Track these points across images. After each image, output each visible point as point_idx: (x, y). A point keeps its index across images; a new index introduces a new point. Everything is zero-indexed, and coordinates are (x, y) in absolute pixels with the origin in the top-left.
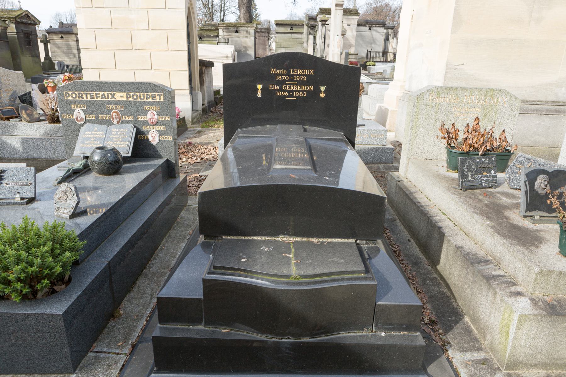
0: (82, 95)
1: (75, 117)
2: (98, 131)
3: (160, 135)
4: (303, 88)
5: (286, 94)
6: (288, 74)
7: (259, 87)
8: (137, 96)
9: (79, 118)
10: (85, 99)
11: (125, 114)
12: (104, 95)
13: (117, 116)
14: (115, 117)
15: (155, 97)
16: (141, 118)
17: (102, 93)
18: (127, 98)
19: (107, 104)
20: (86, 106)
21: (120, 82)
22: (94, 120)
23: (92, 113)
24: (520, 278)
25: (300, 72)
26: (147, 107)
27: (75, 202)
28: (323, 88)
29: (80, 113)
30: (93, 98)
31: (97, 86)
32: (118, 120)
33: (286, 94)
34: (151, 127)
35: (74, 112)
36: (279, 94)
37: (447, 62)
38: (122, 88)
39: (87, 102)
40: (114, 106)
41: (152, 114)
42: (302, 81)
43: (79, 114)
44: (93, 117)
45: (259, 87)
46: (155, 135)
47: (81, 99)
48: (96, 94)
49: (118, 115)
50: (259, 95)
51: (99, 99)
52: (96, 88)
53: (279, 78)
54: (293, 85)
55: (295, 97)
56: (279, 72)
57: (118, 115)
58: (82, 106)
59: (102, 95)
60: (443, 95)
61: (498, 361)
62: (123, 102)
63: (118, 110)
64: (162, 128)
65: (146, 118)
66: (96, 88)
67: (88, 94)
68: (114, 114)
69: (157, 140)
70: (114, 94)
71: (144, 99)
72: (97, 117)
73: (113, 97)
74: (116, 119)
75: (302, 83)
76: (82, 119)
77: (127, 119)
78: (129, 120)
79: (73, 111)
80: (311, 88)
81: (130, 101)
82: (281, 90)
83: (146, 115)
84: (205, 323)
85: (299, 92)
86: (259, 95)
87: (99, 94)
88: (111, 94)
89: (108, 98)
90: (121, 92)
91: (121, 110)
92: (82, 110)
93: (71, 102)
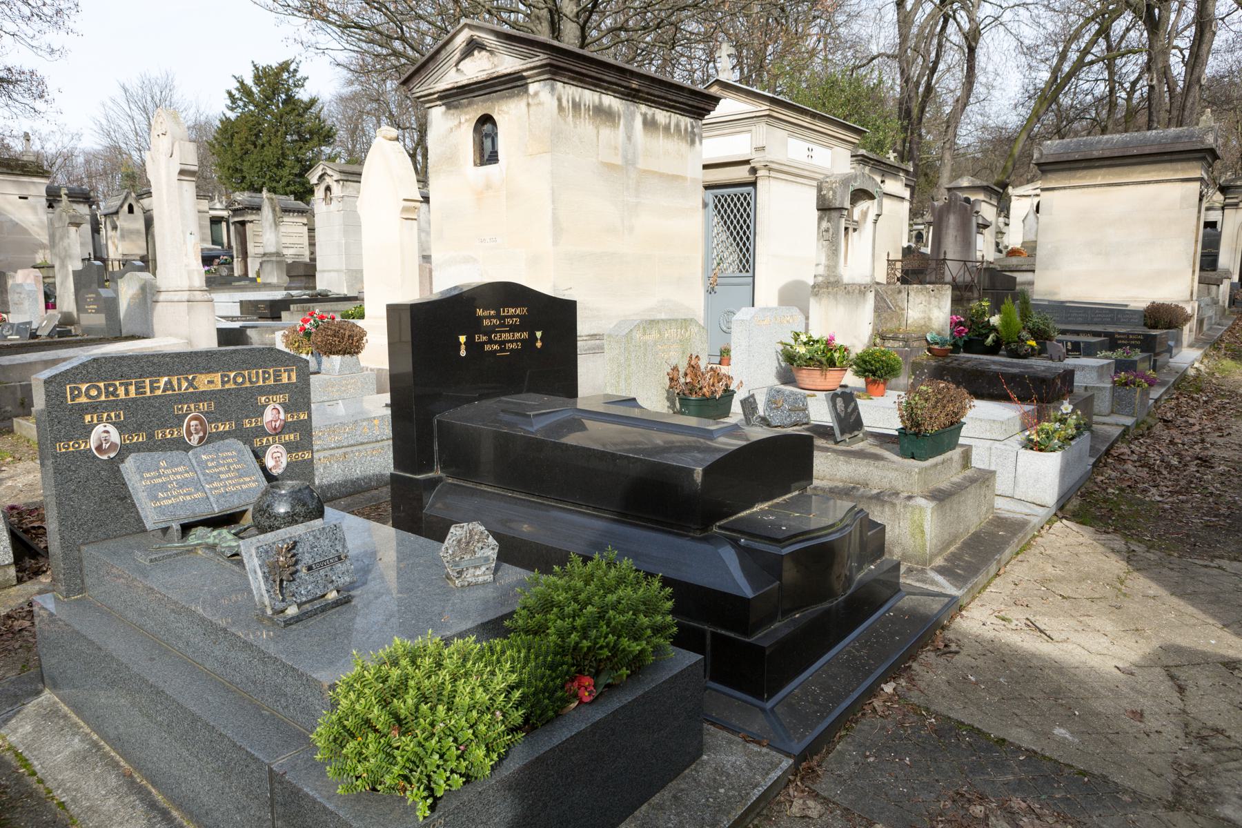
0: (116, 389)
1: (93, 443)
2: (172, 465)
3: (288, 452)
4: (517, 335)
5: (496, 347)
6: (498, 316)
7: (463, 339)
8: (244, 377)
9: (105, 446)
10: (122, 396)
11: (217, 420)
12: (170, 382)
13: (199, 427)
14: (196, 429)
15: (280, 375)
16: (251, 423)
17: (166, 379)
18: (223, 383)
19: (175, 403)
20: (124, 414)
21: (207, 352)
22: (142, 443)
23: (139, 429)
24: (899, 486)
25: (512, 311)
26: (263, 399)
27: (493, 549)
28: (539, 334)
29: (107, 432)
30: (142, 393)
31: (154, 364)
32: (201, 434)
33: (496, 347)
34: (271, 438)
35: (91, 432)
36: (487, 348)
37: (554, 286)
38: (211, 364)
39: (127, 405)
40: (192, 406)
41: (275, 411)
42: (515, 325)
43: (106, 435)
44: (141, 438)
45: (463, 339)
46: (279, 455)
47: (112, 398)
48: (151, 383)
49: (201, 424)
50: (463, 353)
51: (159, 392)
52: (151, 369)
53: (486, 323)
54: (505, 332)
55: (507, 351)
56: (486, 313)
57: (202, 423)
58: (113, 415)
59: (166, 384)
60: (648, 332)
61: (917, 564)
62: (213, 393)
63: (202, 413)
64: (292, 437)
65: (262, 421)
66: (151, 369)
67: (131, 384)
68: (193, 423)
69: (284, 462)
70: (194, 378)
71: (257, 382)
72: (151, 436)
73: (191, 384)
74: (197, 433)
75: (513, 329)
76: (113, 445)
77: (221, 429)
78: (225, 432)
79: (88, 430)
80: (525, 335)
81: (228, 390)
82: (491, 342)
83: (262, 414)
84: (782, 617)
85: (511, 342)
86: (463, 353)
87: (158, 381)
88: (187, 379)
89: (180, 389)
90: (209, 372)
91: (207, 412)
92: (113, 424)
93: (83, 409)
